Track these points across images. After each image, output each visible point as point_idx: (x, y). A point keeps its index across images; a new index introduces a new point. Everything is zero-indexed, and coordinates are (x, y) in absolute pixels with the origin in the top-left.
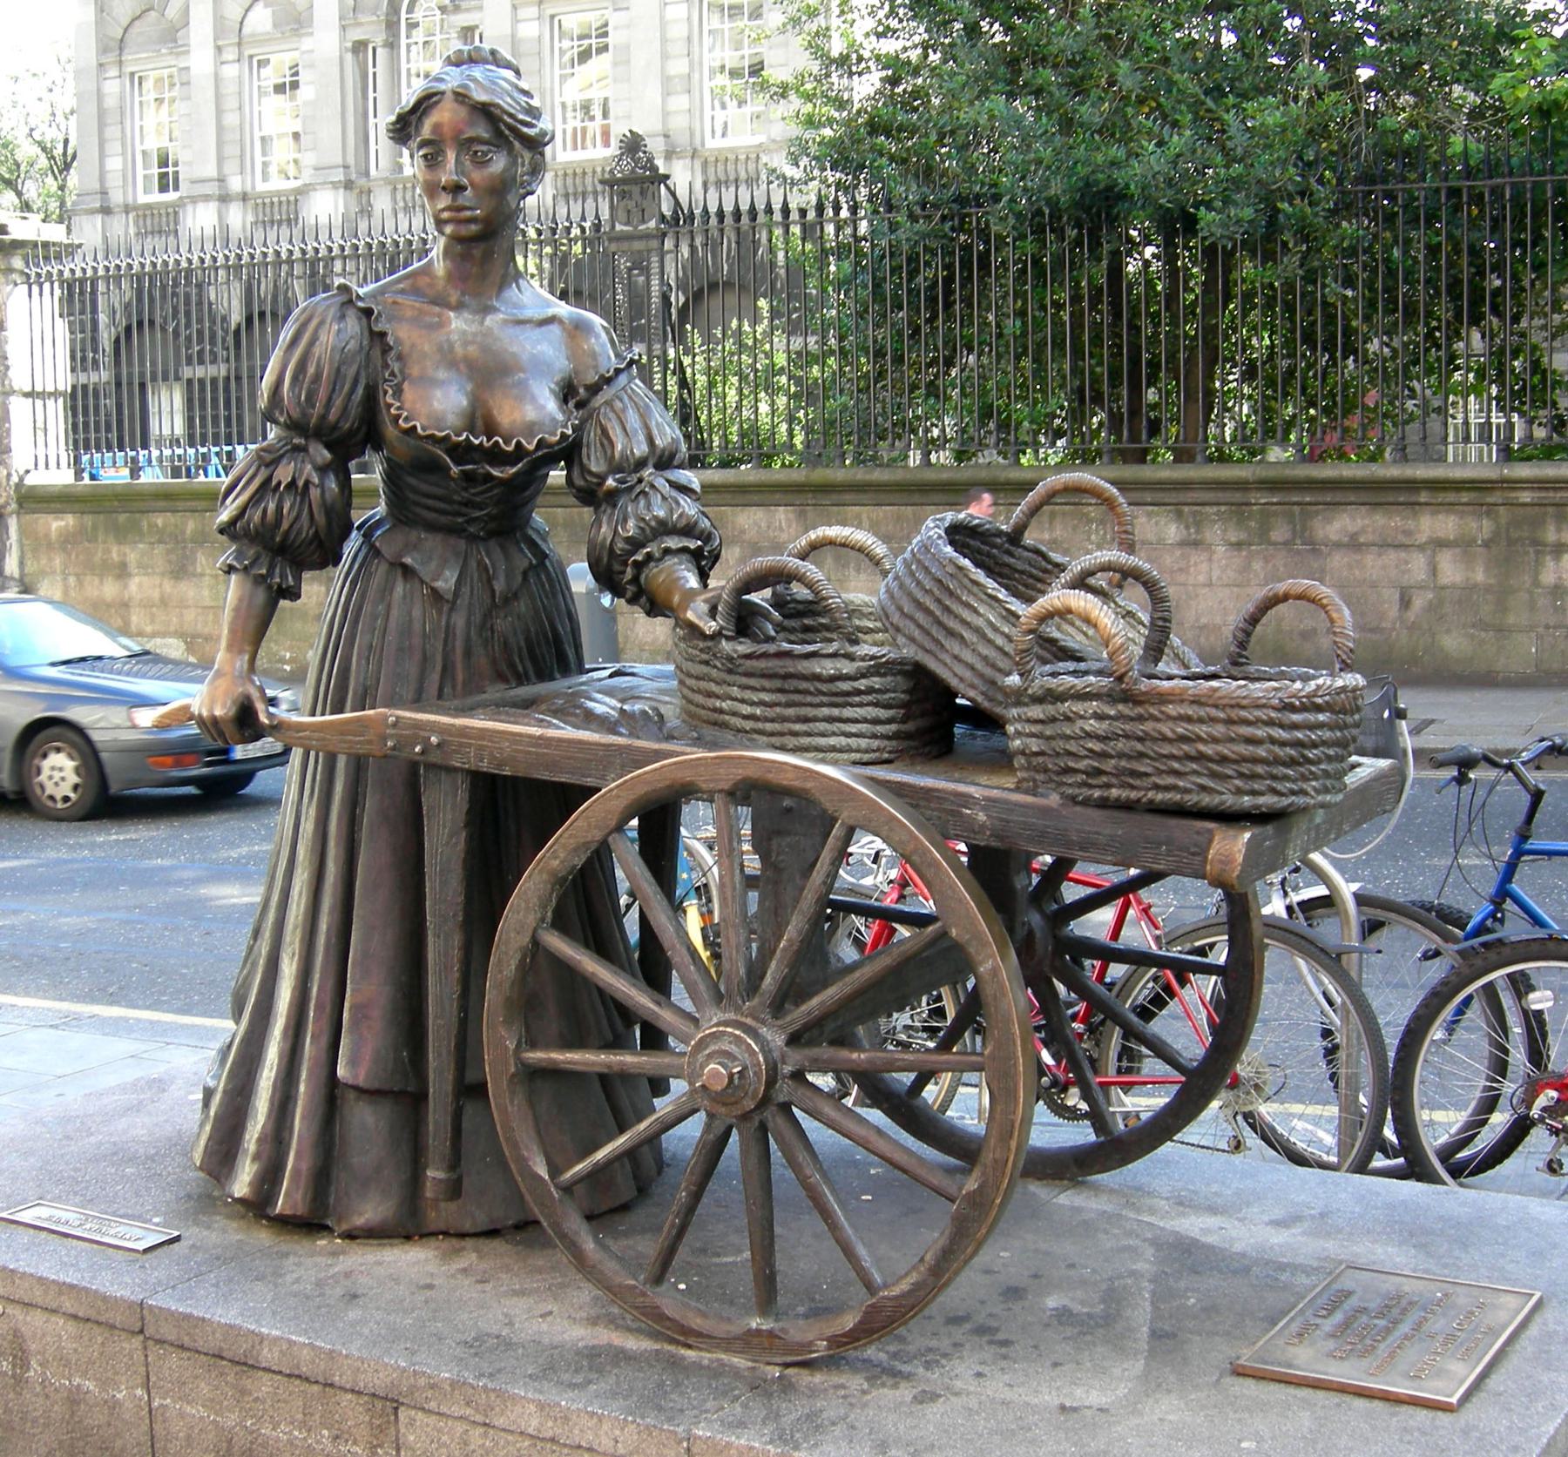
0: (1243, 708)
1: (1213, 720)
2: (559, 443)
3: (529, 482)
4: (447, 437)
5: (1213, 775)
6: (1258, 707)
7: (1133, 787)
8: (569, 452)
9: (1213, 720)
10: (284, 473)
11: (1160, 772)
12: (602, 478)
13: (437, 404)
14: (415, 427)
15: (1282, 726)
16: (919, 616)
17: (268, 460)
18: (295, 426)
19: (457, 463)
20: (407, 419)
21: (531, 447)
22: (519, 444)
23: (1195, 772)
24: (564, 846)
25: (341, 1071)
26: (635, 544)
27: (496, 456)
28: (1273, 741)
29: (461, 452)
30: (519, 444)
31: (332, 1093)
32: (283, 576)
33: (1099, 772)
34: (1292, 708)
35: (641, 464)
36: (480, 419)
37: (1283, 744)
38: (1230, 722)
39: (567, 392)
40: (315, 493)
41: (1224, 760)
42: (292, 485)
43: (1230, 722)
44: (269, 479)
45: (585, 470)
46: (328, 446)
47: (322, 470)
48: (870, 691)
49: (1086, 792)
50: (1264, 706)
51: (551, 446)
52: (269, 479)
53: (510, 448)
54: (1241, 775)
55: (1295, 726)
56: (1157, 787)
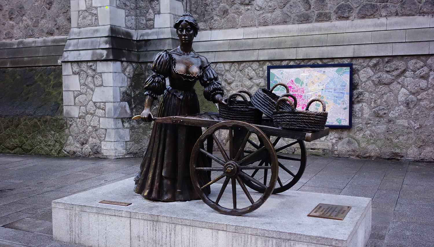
0: (311, 115)
1: (306, 116)
5: (306, 125)
6: (313, 115)
7: (294, 126)
8: (200, 78)
9: (306, 116)
11: (298, 124)
12: (207, 81)
13: (180, 68)
15: (316, 118)
16: (259, 103)
23: (303, 124)
24: (204, 135)
25: (163, 174)
26: (212, 92)
27: (190, 78)
28: (315, 120)
29: (185, 77)
31: (161, 177)
32: (155, 96)
33: (288, 124)
34: (318, 116)
35: (212, 79)
36: (187, 71)
37: (316, 120)
38: (308, 117)
39: (201, 68)
41: (307, 122)
43: (308, 117)
44: (154, 80)
45: (203, 80)
48: (250, 113)
49: (286, 127)
50: (314, 115)
52: (154, 80)
54: (310, 125)
55: (318, 118)
56: (297, 126)
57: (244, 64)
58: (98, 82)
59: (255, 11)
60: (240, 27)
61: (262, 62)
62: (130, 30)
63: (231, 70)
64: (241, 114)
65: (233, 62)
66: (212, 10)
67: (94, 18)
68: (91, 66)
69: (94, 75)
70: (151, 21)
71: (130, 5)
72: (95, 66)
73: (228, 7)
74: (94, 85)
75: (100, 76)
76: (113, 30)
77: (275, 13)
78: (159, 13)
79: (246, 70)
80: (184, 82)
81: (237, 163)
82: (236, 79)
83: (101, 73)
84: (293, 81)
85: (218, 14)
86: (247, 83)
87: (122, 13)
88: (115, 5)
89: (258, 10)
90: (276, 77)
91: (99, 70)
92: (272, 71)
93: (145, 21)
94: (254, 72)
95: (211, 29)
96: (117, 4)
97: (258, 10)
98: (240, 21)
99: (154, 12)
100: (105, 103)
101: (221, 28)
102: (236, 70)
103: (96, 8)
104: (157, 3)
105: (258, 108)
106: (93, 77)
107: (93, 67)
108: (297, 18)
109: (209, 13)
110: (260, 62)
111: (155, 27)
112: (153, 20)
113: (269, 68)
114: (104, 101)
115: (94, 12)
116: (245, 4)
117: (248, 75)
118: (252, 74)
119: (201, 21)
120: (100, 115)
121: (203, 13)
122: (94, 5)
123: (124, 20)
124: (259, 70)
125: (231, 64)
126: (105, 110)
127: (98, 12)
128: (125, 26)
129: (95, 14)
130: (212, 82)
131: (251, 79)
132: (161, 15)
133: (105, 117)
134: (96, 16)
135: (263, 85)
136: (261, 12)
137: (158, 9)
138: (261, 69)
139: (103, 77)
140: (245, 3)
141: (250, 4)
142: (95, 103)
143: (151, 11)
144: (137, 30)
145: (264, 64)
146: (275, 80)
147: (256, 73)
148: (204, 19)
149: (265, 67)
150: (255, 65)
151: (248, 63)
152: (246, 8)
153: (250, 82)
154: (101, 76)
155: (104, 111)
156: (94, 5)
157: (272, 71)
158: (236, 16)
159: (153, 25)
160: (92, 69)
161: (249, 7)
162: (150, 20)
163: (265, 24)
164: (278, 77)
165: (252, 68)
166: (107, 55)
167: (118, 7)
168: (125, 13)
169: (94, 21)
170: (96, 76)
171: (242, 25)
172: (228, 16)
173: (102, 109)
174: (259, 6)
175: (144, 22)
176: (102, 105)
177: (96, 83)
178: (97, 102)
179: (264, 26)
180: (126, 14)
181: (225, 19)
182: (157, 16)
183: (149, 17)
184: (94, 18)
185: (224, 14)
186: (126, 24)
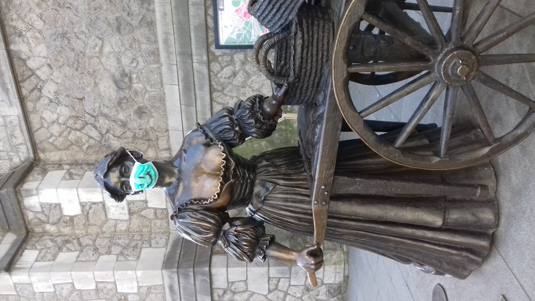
2: (224, 146)
3: (240, 162)
4: (221, 183)
8: (229, 145)
10: (233, 239)
12: (236, 132)
14: (217, 194)
17: (228, 243)
18: (217, 235)
19: (230, 180)
20: (215, 196)
21: (225, 155)
22: (223, 159)
24: (365, 135)
26: (257, 120)
27: (227, 167)
29: (225, 178)
30: (223, 159)
35: (231, 119)
40: (239, 229)
42: (236, 236)
44: (233, 243)
46: (224, 224)
47: (232, 225)
51: (225, 149)
52: (233, 243)
53: (225, 161)
57: (213, 83)
58: (241, 286)
59: (139, 67)
60: (162, 89)
61: (210, 57)
62: (171, 241)
63: (223, 102)
64: (310, 50)
65: (211, 99)
66: (140, 129)
67: (153, 291)
68: (219, 296)
69: (232, 291)
70: (157, 213)
71: (137, 240)
72: (218, 290)
73: (136, 107)
74: (245, 291)
75: (232, 285)
76: (168, 264)
77: (140, 38)
78: (146, 202)
79: (222, 80)
80: (239, 177)
81: (442, 50)
82: (235, 95)
83: (228, 283)
84: (237, 10)
85: (146, 120)
86: (240, 79)
87: (146, 252)
88: (134, 263)
89: (138, 63)
90: (232, 36)
91: (224, 285)
92: (222, 42)
93: (157, 221)
94: (225, 70)
95: (167, 131)
96: (133, 259)
97: (138, 63)
98: (153, 90)
99: (145, 209)
100: (269, 278)
101: (165, 116)
102: (222, 96)
103: (139, 288)
104: (132, 204)
105: (296, 10)
106: (234, 293)
107: (221, 292)
108: (146, 5)
109: (145, 133)
110: (211, 60)
111: (165, 207)
112: (156, 209)
113: (219, 47)
114: (267, 279)
115: (144, 290)
116: (130, 83)
117: (229, 78)
118: (227, 71)
119: (157, 144)
120: (287, 284)
121: (146, 142)
122: (135, 291)
123: (156, 249)
124: (222, 61)
125: (213, 103)
126: (280, 278)
127: (144, 285)
128: (165, 248)
129: (148, 289)
130: (236, 120)
131: (234, 74)
132: (148, 199)
133: (290, 278)
134: (151, 288)
135: (243, 56)
136: (140, 59)
137: (140, 203)
138: (220, 59)
139: (234, 280)
140: (129, 83)
141: (129, 75)
142: (270, 291)
143: (143, 213)
144: (171, 231)
145: (213, 54)
146: (235, 38)
147: (226, 66)
148: (153, 139)
149: (218, 52)
150: (215, 67)
151: (212, 78)
152: (135, 81)
153: (238, 76)
154: (233, 283)
155: (281, 280)
156: (135, 291)
157: (222, 42)
158: (147, 96)
159: (162, 209)
160: (223, 295)
161: (134, 76)
162: (156, 213)
163: (155, 53)
164: (232, 33)
165: (219, 72)
166: (203, 274)
167: (138, 257)
168: (146, 247)
169: (157, 291)
170: (233, 290)
171: (159, 86)
172: (148, 106)
173: (279, 282)
174: (132, 62)
175: (158, 222)
176: (275, 281)
177: (242, 290)
178: (269, 288)
179: (159, 55)
180: (148, 246)
181: (152, 110)
182: (150, 205)
183: (152, 216)
184: (153, 291)
185: (145, 113)
186: (162, 247)
